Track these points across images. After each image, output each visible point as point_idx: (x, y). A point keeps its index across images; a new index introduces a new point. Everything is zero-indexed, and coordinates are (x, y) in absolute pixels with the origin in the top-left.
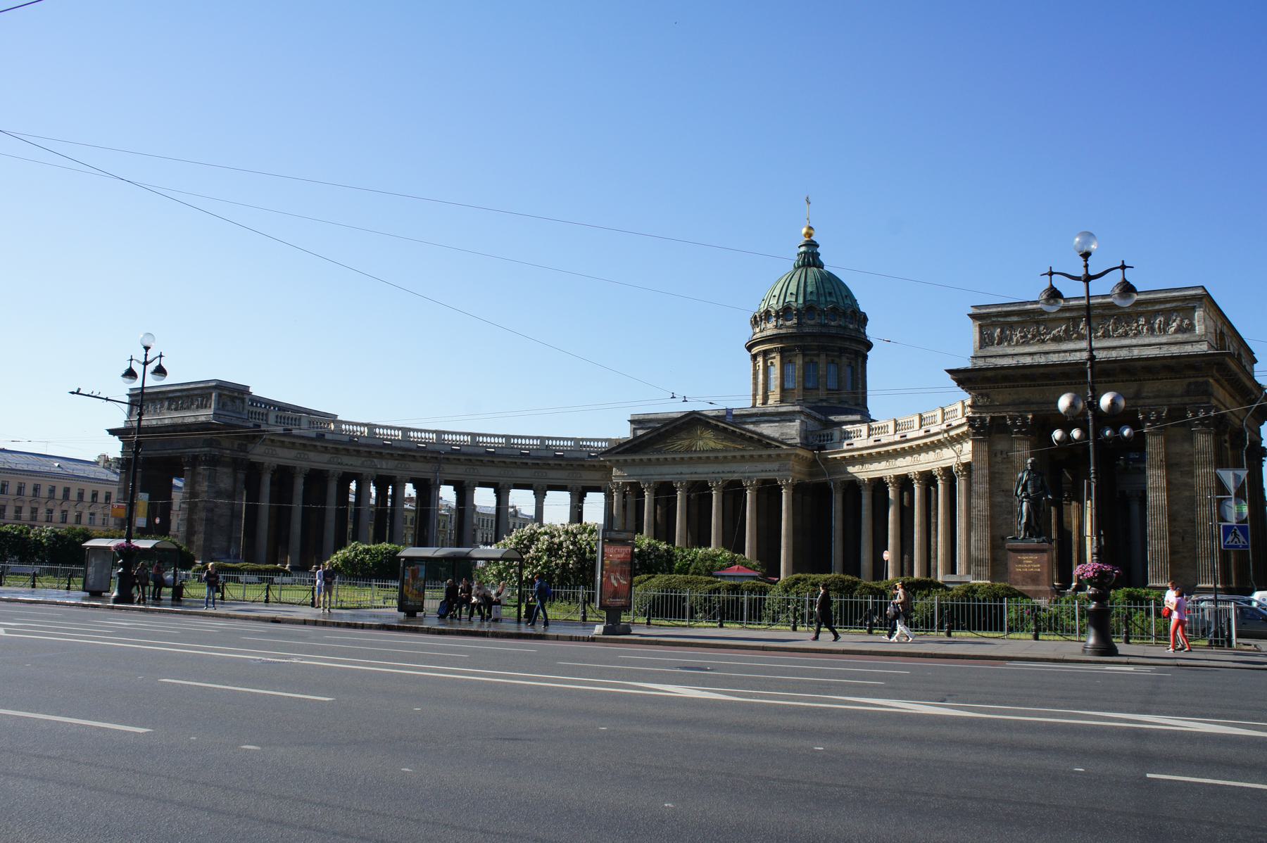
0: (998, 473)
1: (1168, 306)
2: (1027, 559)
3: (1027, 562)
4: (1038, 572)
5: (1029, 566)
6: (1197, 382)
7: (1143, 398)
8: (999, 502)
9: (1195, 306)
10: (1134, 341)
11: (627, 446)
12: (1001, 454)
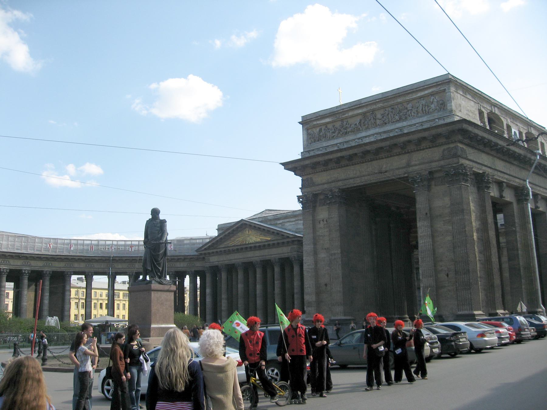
0: (322, 236)
1: (426, 92)
6: (448, 148)
9: (445, 89)
10: (405, 124)
11: (210, 244)
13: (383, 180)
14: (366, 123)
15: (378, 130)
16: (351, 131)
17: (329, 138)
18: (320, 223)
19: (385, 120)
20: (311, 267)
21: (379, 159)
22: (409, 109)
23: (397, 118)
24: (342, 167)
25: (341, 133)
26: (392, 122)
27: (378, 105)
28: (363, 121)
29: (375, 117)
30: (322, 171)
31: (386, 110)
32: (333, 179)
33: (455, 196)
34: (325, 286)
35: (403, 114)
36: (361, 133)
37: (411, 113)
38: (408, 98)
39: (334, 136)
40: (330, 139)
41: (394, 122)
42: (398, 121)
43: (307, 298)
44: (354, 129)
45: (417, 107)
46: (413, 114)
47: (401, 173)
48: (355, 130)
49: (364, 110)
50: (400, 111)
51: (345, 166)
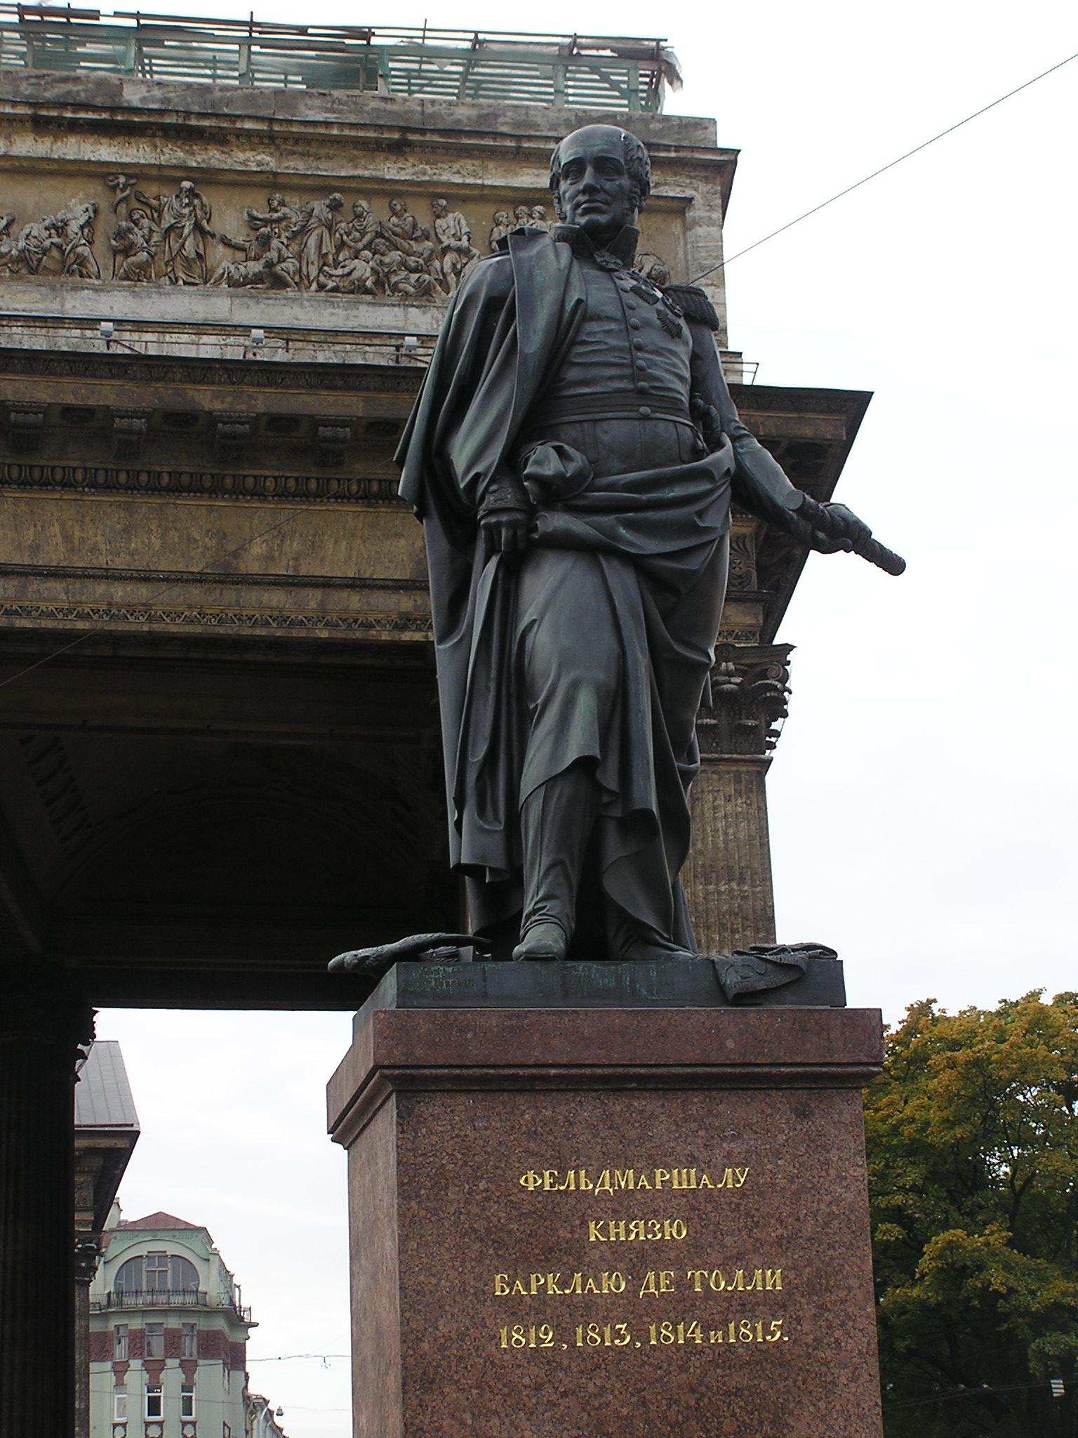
3: (637, 1231)
4: (762, 1355)
5: (658, 1282)
9: (690, 200)
15: (220, 307)
19: (281, 259)
21: (239, 491)
22: (446, 242)
23: (362, 269)
26: (321, 287)
27: (241, 156)
28: (105, 225)
29: (204, 222)
31: (282, 203)
33: (720, 825)
35: (403, 264)
36: (96, 290)
38: (452, 174)
41: (335, 289)
42: (367, 292)
44: (45, 252)
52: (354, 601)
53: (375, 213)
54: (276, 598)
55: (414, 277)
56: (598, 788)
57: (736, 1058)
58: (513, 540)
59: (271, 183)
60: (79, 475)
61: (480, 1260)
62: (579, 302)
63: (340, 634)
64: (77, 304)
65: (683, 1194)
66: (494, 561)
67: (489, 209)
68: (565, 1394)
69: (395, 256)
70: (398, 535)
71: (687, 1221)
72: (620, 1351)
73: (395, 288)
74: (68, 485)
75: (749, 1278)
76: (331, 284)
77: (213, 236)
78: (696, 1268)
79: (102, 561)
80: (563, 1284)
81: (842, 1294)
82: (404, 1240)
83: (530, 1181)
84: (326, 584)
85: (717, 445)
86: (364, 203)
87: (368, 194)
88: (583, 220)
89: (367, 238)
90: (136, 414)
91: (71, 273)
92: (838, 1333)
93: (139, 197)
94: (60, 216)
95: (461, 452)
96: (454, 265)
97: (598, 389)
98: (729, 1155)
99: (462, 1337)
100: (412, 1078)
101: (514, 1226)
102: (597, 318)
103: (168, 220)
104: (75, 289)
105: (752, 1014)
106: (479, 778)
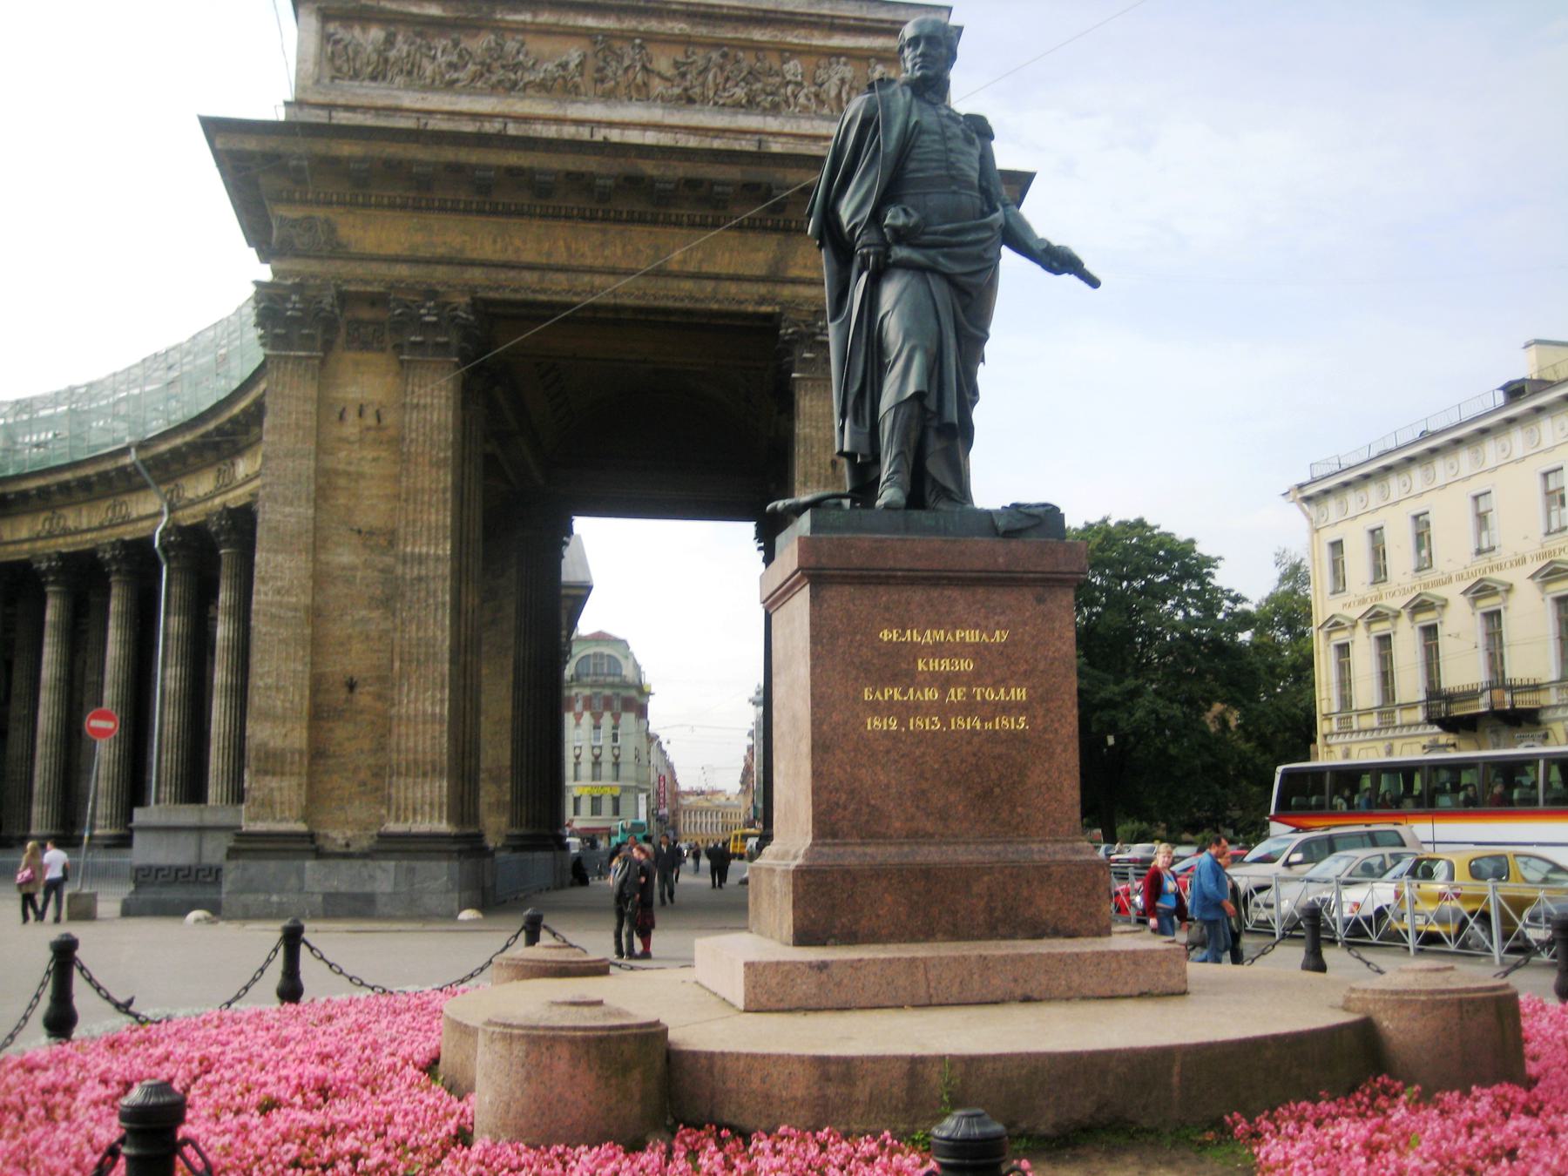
0: (348, 474)
1: (864, 42)
2: (938, 650)
3: (945, 665)
4: (1014, 736)
5: (957, 694)
7: (795, 281)
8: (344, 568)
10: (772, 124)
12: (361, 414)
13: (670, 304)
14: (609, 72)
15: (657, 114)
16: (544, 88)
17: (428, 81)
18: (341, 417)
20: (294, 600)
21: (667, 223)
22: (789, 77)
23: (740, 93)
24: (494, 212)
25: (494, 79)
26: (716, 104)
30: (392, 206)
31: (693, 53)
32: (441, 251)
34: (346, 689)
35: (763, 91)
36: (586, 103)
37: (795, 97)
38: (794, 38)
39: (457, 81)
40: (430, 88)
41: (724, 105)
42: (742, 106)
43: (259, 733)
44: (555, 80)
45: (819, 81)
46: (802, 100)
47: (748, 298)
48: (556, 86)
49: (609, 23)
50: (753, 75)
51: (509, 212)
52: (733, 288)
53: (747, 60)
54: (688, 285)
55: (770, 98)
56: (924, 409)
57: (1003, 568)
58: (876, 263)
59: (686, 41)
60: (575, 212)
61: (856, 679)
62: (917, 123)
63: (726, 306)
64: (575, 111)
65: (972, 645)
66: (864, 276)
67: (814, 59)
68: (903, 756)
69: (758, 86)
70: (759, 250)
71: (974, 661)
72: (935, 733)
73: (758, 104)
74: (568, 217)
75: (1007, 693)
76: (721, 102)
77: (653, 72)
78: (978, 686)
79: (588, 262)
80: (903, 693)
81: (1060, 703)
82: (813, 667)
83: (885, 635)
84: (716, 277)
85: (995, 210)
86: (741, 54)
87: (743, 48)
88: (918, 74)
89: (742, 75)
90: (608, 177)
91: (570, 92)
92: (1056, 725)
93: (610, 48)
94: (564, 58)
95: (845, 210)
96: (793, 93)
97: (927, 174)
98: (998, 623)
99: (846, 723)
100: (820, 576)
101: (875, 661)
102: (928, 132)
103: (627, 62)
104: (574, 102)
105: (1014, 544)
106: (855, 402)
